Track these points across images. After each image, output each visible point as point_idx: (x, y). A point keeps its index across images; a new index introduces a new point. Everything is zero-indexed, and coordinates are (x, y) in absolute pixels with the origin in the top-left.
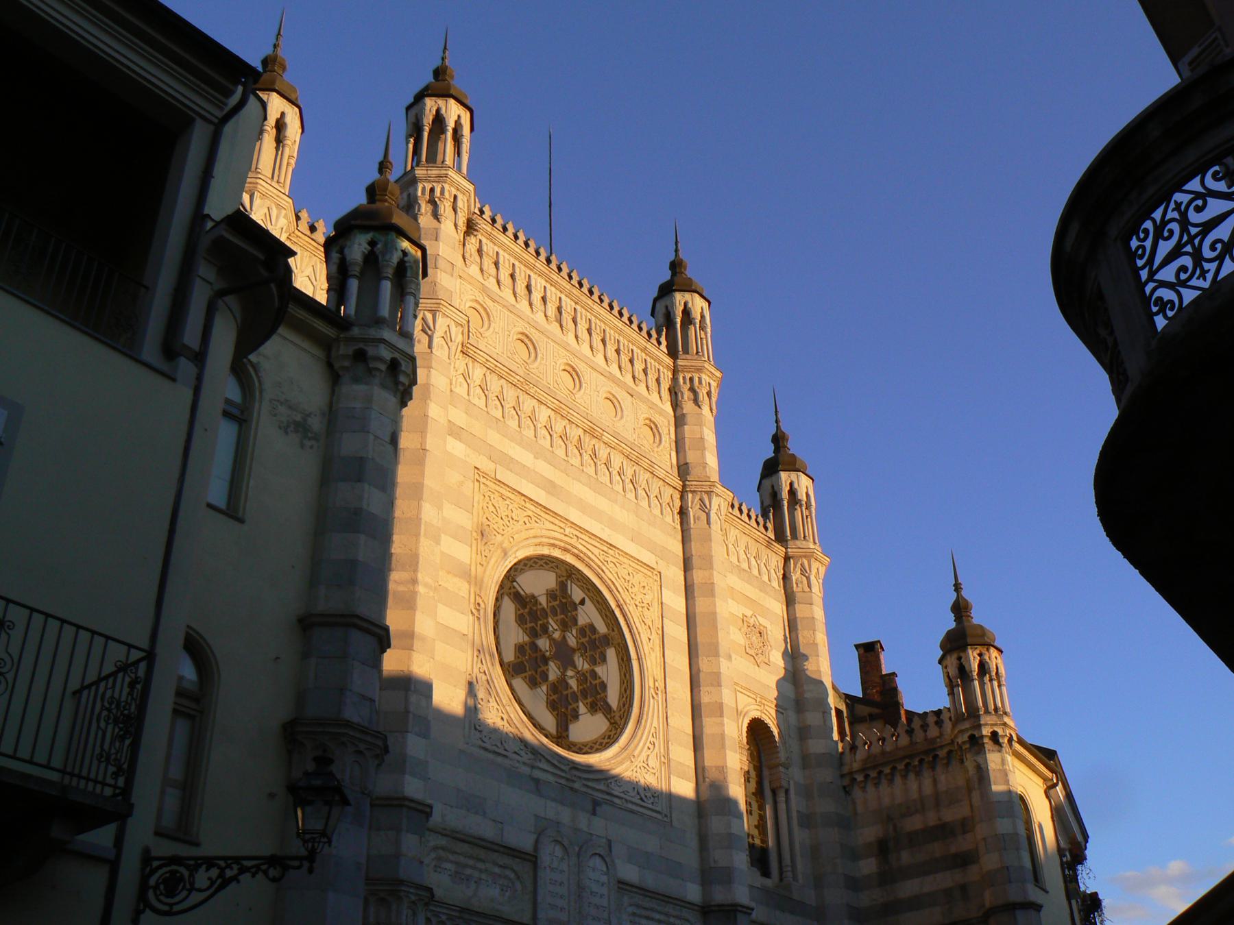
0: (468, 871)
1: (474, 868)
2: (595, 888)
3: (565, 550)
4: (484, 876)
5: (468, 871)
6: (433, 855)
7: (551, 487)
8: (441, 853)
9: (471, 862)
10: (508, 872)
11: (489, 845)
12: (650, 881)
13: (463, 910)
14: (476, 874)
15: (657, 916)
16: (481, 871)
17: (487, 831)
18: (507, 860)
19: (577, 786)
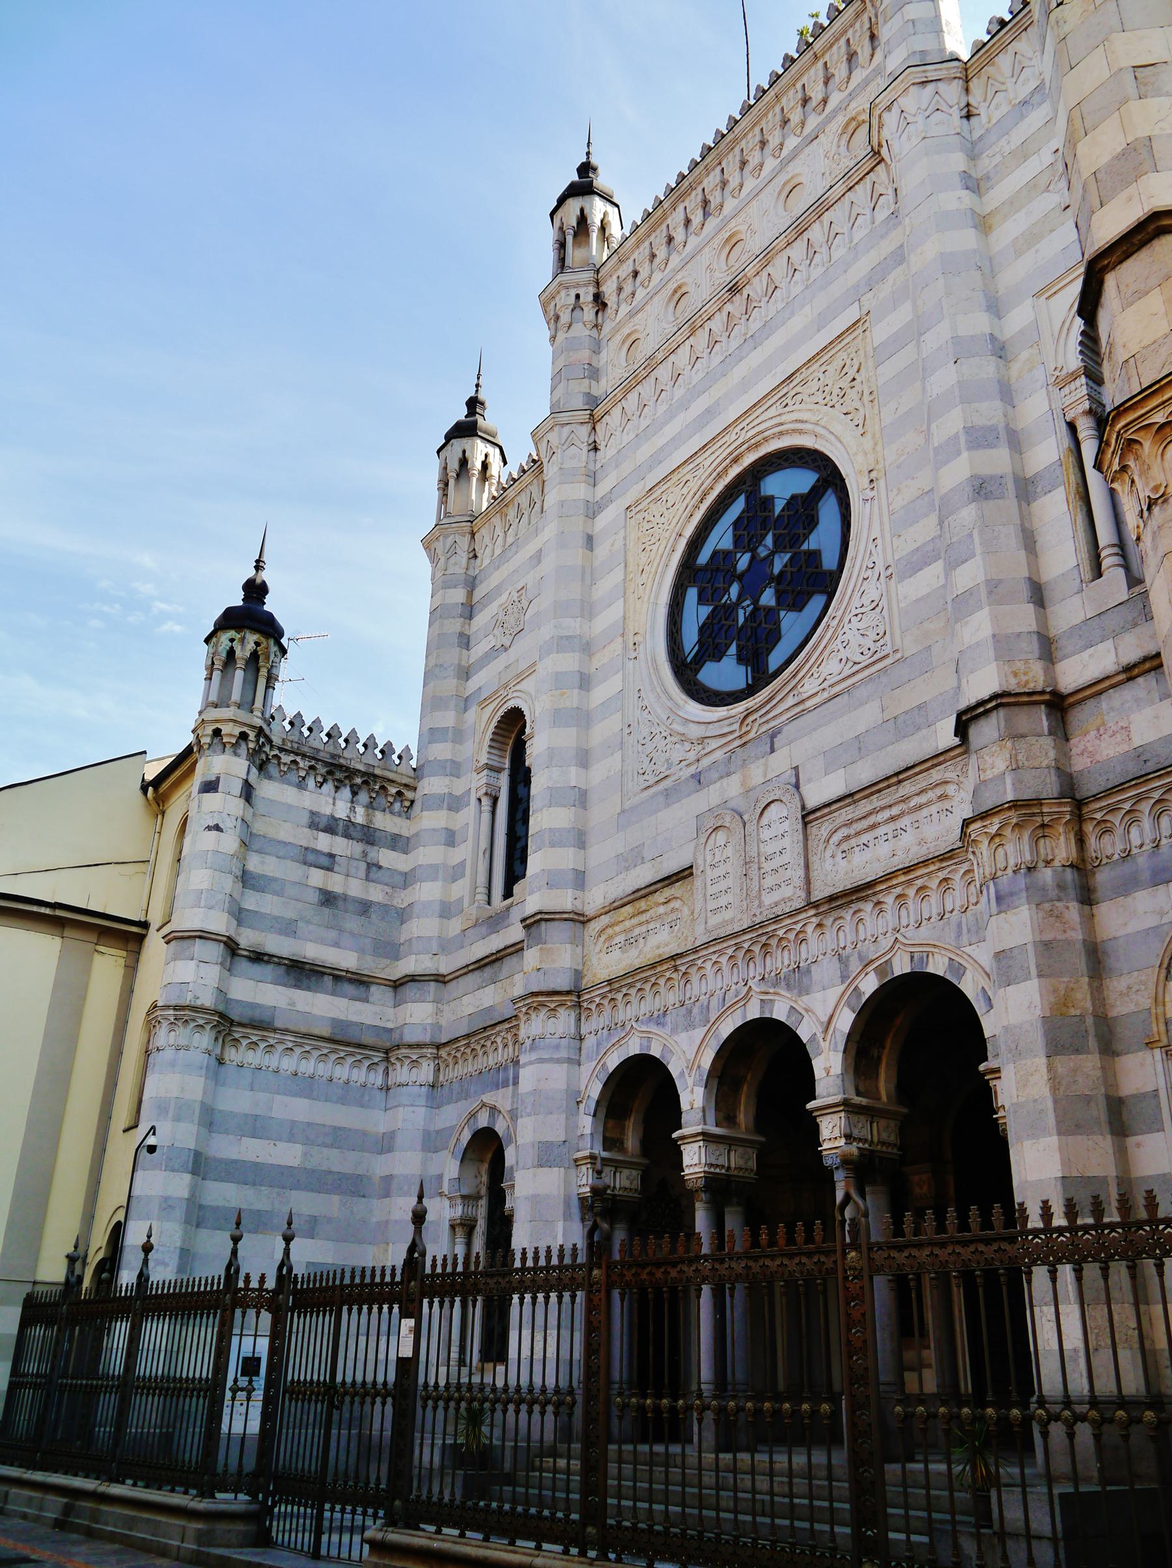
0: (637, 931)
1: (640, 924)
2: (768, 849)
3: (736, 460)
4: (651, 926)
5: (637, 931)
6: (602, 939)
7: (710, 413)
8: (610, 931)
9: (635, 921)
10: (672, 905)
11: (647, 890)
12: (866, 773)
13: (610, 982)
14: (644, 928)
15: (886, 814)
16: (647, 922)
17: (644, 875)
18: (667, 892)
19: (752, 735)
